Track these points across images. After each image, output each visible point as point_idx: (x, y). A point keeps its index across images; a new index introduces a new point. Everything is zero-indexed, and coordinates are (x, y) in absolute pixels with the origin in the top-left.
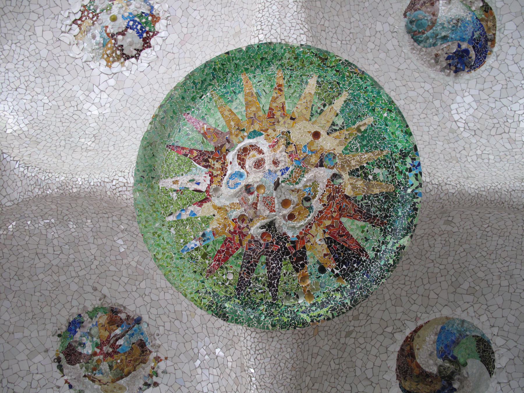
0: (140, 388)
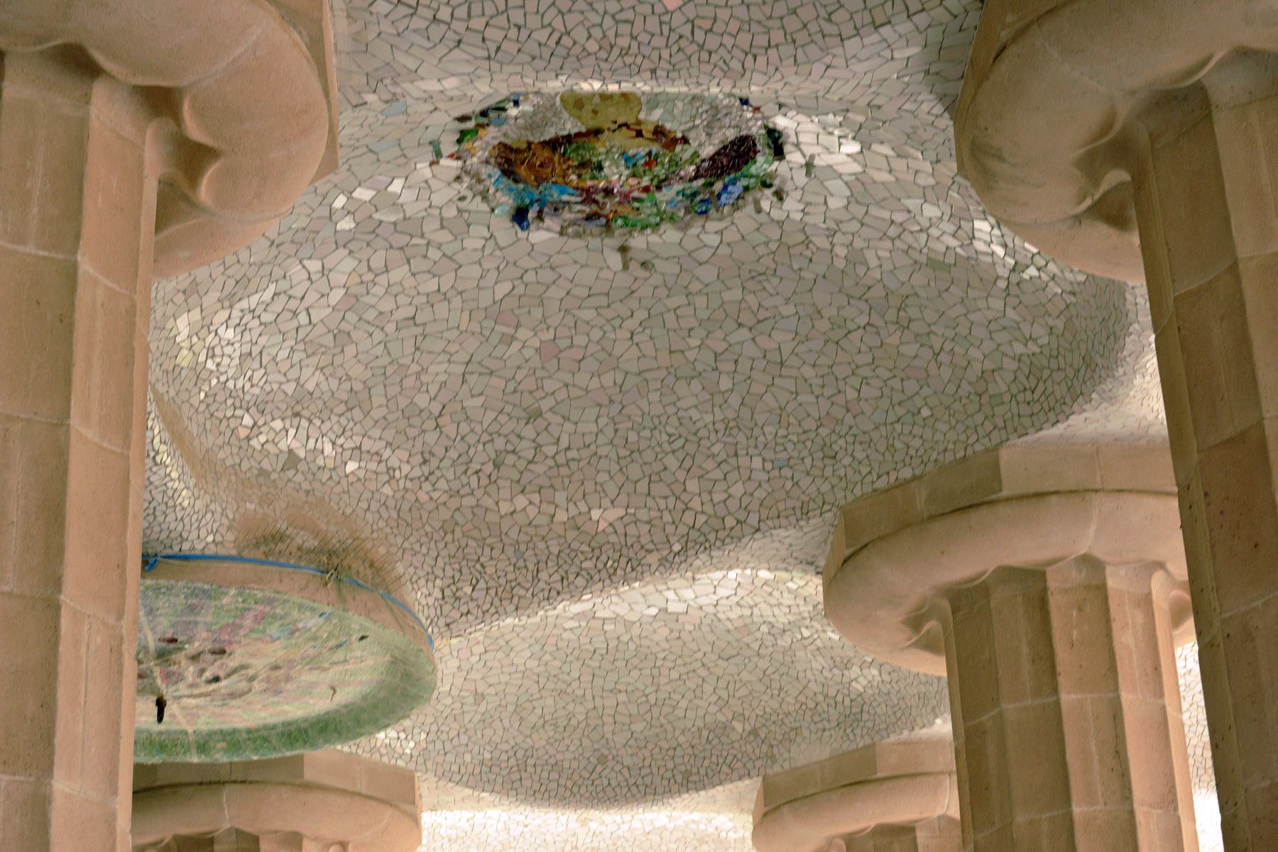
0: (516, 103)
